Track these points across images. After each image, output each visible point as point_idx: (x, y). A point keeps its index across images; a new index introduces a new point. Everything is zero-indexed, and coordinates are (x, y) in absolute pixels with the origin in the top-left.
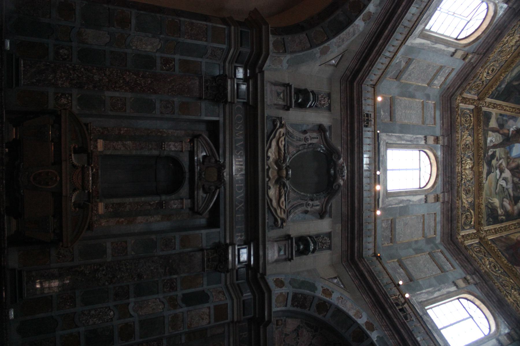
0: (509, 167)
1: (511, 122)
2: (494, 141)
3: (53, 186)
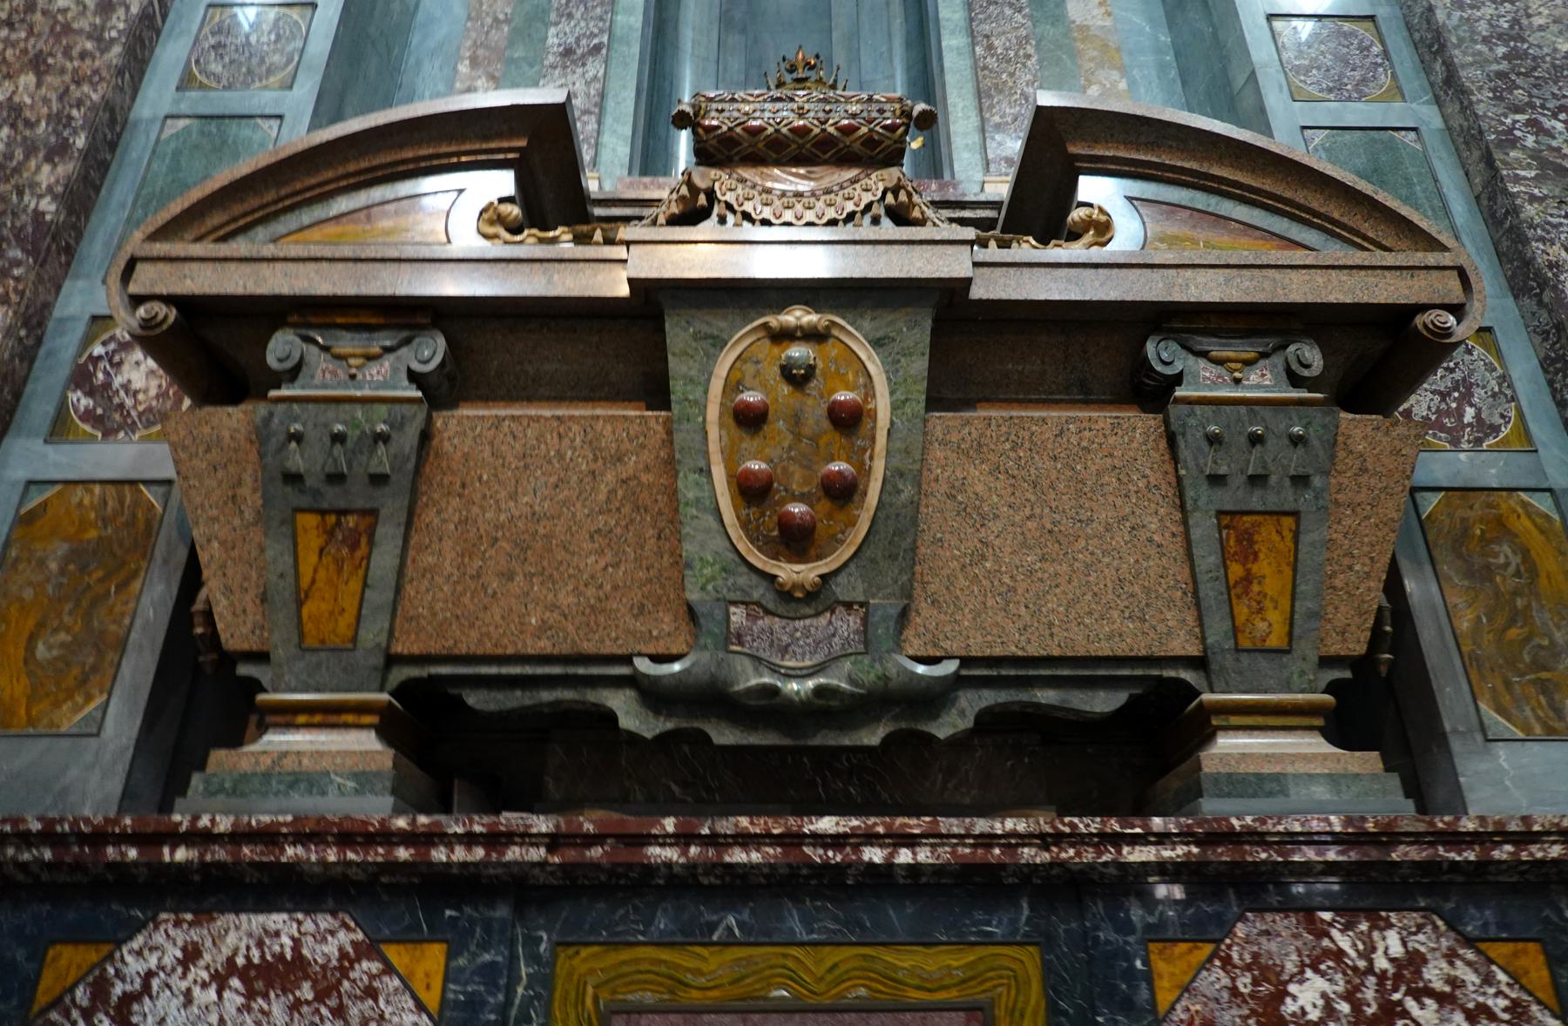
3: (875, 367)
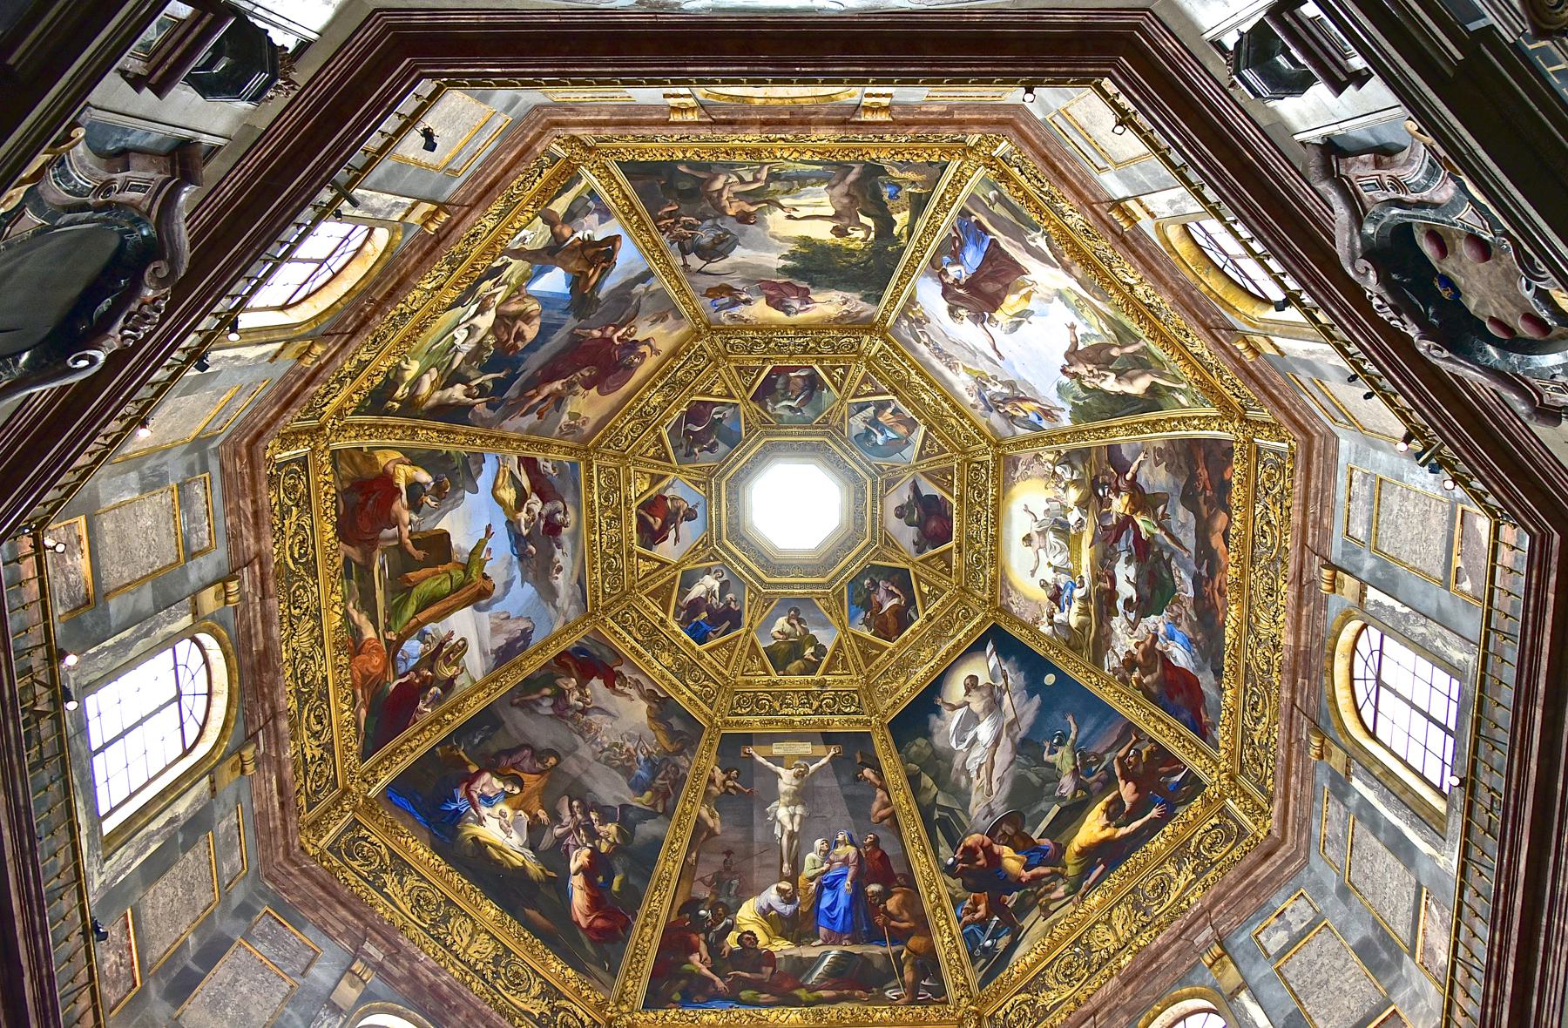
0: (501, 308)
1: (593, 218)
2: (528, 240)
